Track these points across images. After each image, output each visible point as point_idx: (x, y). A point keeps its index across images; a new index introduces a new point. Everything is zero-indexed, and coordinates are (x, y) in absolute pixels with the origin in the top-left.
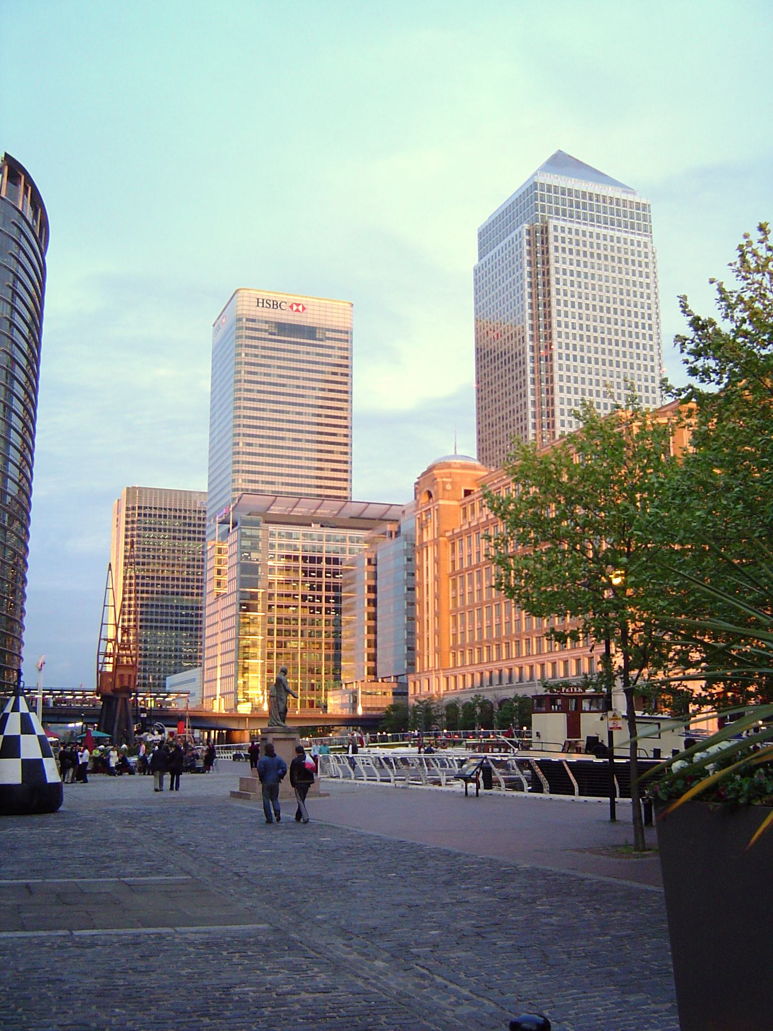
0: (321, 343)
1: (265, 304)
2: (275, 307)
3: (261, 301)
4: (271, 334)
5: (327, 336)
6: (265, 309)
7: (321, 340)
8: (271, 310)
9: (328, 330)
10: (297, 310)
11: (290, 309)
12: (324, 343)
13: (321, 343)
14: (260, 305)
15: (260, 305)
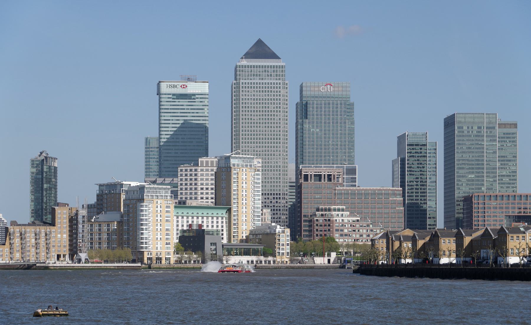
0: (194, 100)
1: (170, 87)
2: (174, 87)
3: (168, 85)
4: (173, 99)
5: (196, 97)
6: (170, 89)
7: (195, 99)
8: (173, 89)
9: (197, 94)
10: (184, 88)
11: (181, 87)
12: (195, 100)
13: (194, 100)
14: (168, 87)
15: (168, 87)
